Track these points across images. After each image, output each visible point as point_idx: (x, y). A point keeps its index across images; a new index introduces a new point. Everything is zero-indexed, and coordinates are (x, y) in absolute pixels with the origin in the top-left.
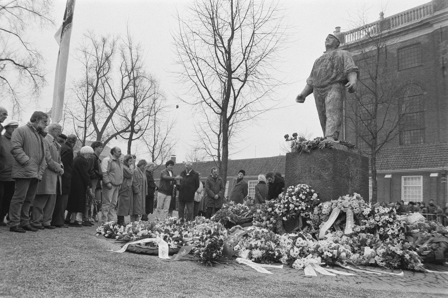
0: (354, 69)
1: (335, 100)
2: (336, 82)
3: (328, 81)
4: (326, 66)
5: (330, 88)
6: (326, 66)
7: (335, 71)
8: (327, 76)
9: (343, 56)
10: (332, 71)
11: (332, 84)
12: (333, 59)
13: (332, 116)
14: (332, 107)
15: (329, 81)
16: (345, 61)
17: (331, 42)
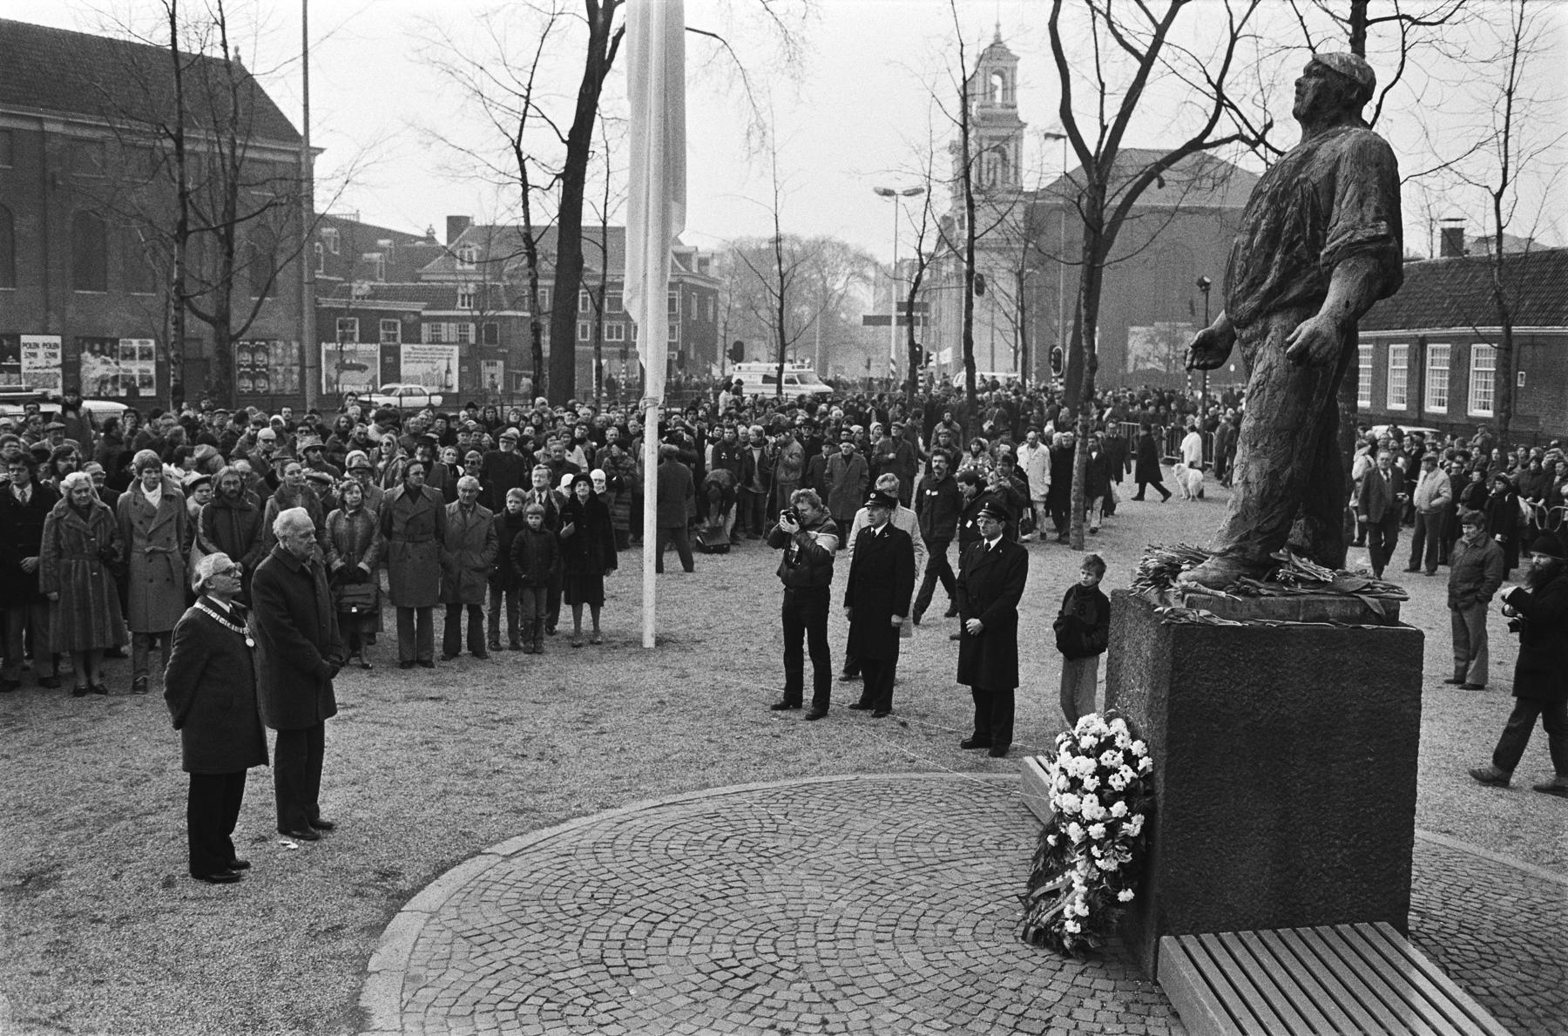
0: (1359, 242)
1: (1267, 393)
2: (1283, 308)
3: (1250, 304)
4: (1253, 232)
5: (1265, 332)
6: (1253, 232)
7: (1278, 257)
8: (1246, 280)
9: (1332, 176)
10: (1270, 257)
11: (1269, 314)
12: (1286, 194)
13: (1247, 465)
14: (1251, 424)
15: (1254, 304)
16: (1337, 198)
17: (1309, 97)
